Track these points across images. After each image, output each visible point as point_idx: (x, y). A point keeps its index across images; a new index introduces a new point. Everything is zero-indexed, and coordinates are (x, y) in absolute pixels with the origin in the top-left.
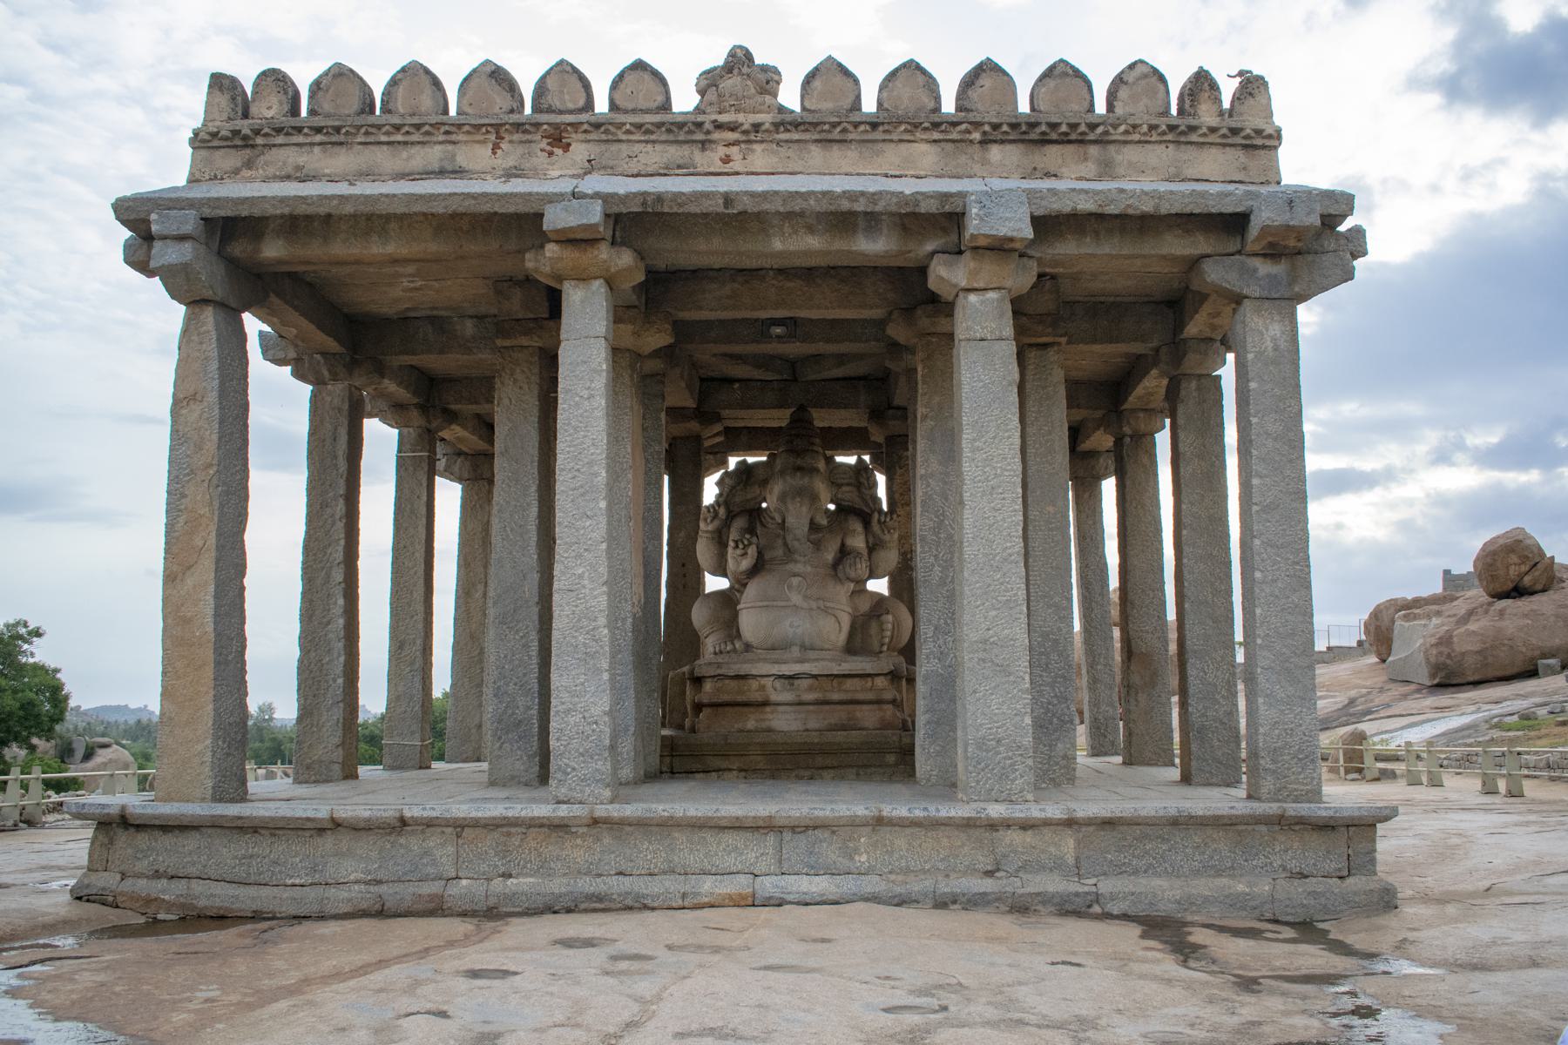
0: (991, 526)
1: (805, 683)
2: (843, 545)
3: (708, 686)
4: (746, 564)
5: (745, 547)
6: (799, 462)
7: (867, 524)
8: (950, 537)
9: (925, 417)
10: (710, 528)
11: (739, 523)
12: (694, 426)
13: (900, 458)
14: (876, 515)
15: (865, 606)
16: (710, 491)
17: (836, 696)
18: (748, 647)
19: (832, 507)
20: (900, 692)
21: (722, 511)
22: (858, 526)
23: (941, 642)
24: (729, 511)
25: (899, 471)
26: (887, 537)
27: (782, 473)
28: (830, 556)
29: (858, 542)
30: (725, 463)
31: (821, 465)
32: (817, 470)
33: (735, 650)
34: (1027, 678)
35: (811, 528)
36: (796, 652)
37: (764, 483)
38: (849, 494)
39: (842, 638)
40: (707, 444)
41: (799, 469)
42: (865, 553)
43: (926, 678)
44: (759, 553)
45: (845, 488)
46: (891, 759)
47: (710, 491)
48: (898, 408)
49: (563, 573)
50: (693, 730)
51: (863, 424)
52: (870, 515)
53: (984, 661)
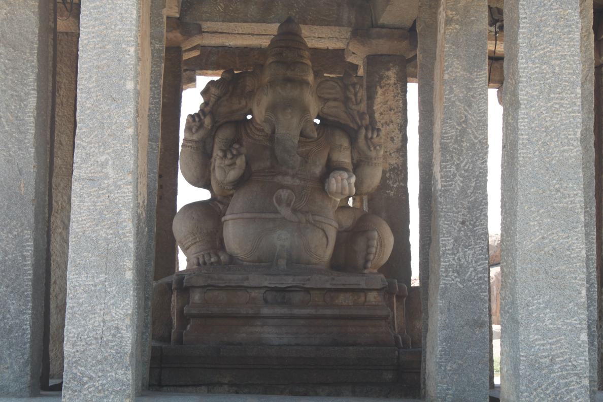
0: (547, 128)
1: (297, 297)
2: (329, 160)
3: (196, 297)
4: (233, 175)
5: (234, 156)
6: (289, 73)
7: (353, 141)
8: (474, 144)
9: (449, 21)
10: (195, 137)
11: (224, 134)
12: (177, 35)
13: (381, 78)
14: (363, 131)
15: (348, 221)
16: (192, 101)
17: (328, 312)
18: (232, 259)
19: (317, 121)
20: (392, 310)
21: (207, 121)
22: (345, 143)
23: (461, 254)
24: (214, 122)
25: (380, 91)
26: (373, 154)
27: (272, 84)
28: (318, 170)
29: (344, 157)
30: (192, 80)
31: (310, 78)
32: (308, 83)
33: (219, 262)
34: (584, 293)
35: (299, 142)
36: (282, 263)
37: (251, 94)
38: (335, 109)
39: (329, 252)
40: (186, 56)
41: (288, 80)
42: (350, 168)
43: (445, 290)
44: (248, 164)
45: (332, 104)
46: (388, 376)
47: (192, 101)
48: (383, 26)
49: (84, 161)
50: (180, 341)
51: (339, 45)
52: (357, 132)
53: (537, 271)
